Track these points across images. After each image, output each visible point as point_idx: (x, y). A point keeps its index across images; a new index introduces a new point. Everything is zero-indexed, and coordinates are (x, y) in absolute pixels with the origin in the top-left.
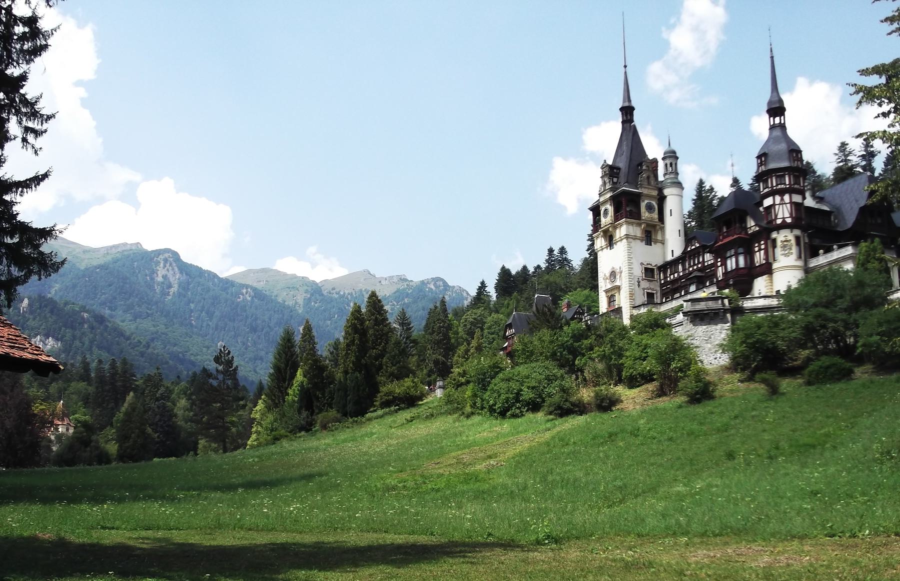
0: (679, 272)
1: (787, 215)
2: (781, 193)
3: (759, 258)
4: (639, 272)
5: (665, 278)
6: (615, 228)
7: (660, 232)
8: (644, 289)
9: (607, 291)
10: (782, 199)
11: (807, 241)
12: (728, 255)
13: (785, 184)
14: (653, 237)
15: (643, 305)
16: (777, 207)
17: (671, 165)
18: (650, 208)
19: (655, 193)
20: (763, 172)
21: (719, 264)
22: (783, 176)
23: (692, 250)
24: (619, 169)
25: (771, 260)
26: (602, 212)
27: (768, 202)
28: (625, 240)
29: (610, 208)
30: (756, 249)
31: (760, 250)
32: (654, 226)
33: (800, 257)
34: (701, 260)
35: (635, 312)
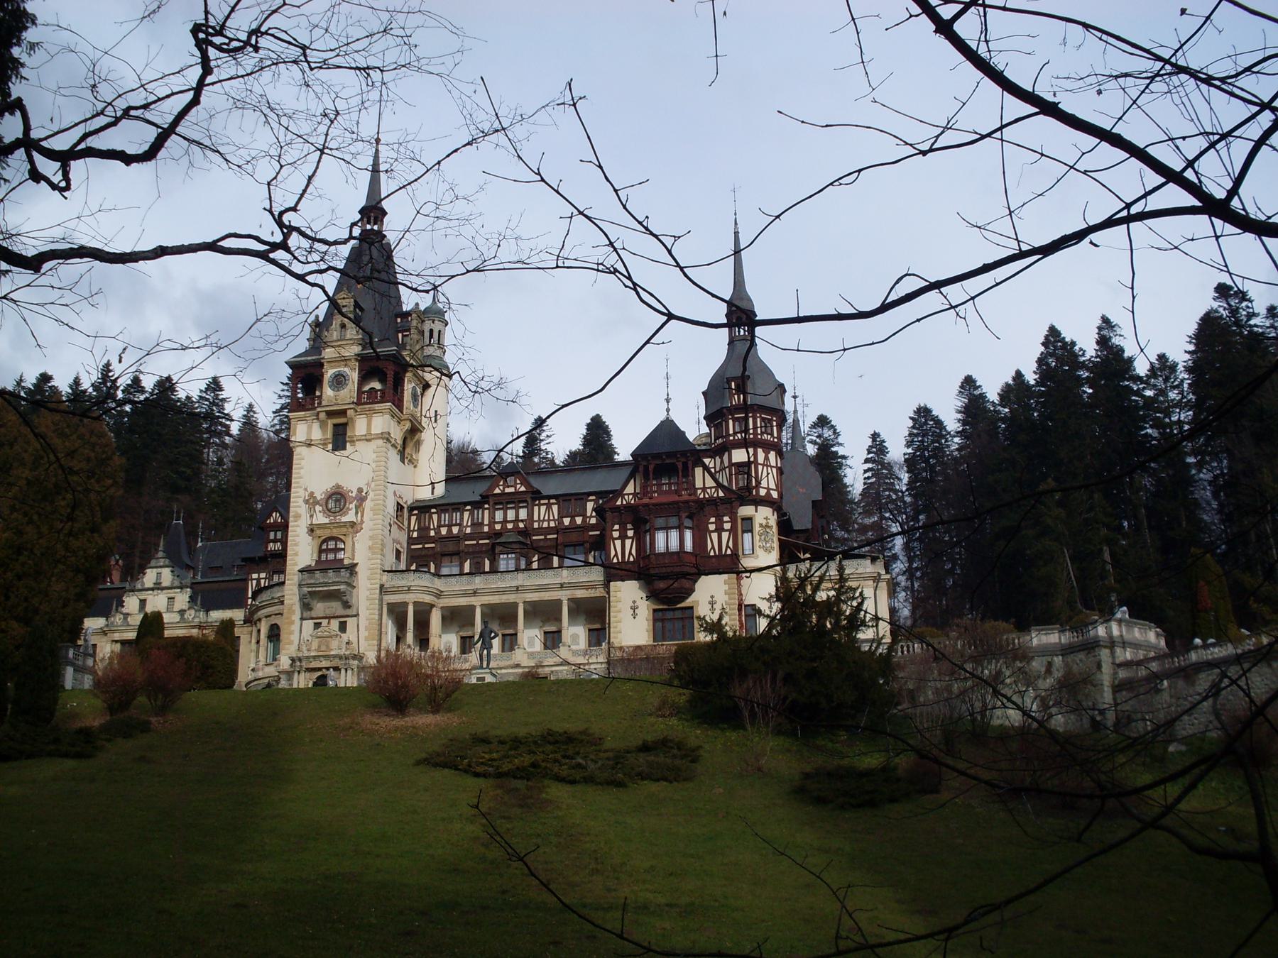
0: (460, 525)
1: (772, 486)
2: (768, 447)
5: (423, 530)
10: (766, 458)
13: (772, 434)
16: (760, 467)
18: (414, 397)
21: (616, 534)
22: (770, 421)
23: (503, 494)
24: (362, 310)
27: (739, 456)
28: (380, 442)
29: (354, 376)
30: (712, 527)
31: (720, 530)
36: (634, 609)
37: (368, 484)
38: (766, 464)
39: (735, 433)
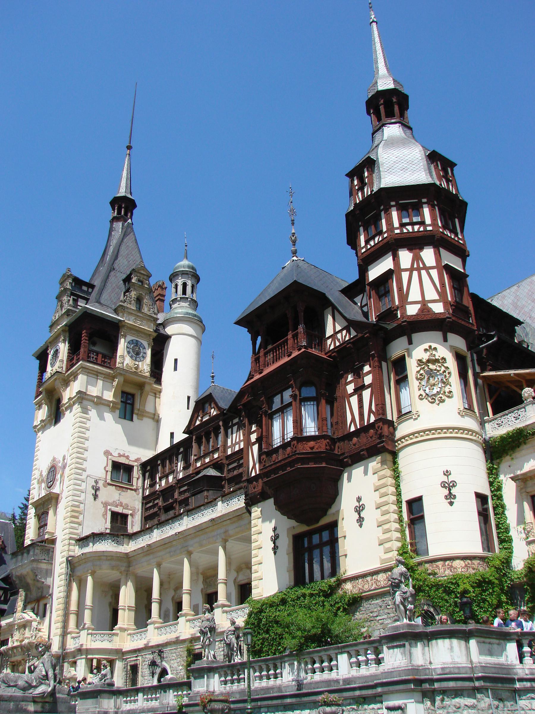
1: (431, 294)
2: (415, 243)
3: (357, 409)
4: (98, 468)
5: (152, 485)
6: (66, 383)
7: (150, 398)
8: (106, 504)
9: (37, 505)
10: (417, 258)
11: (478, 370)
12: (275, 407)
13: (422, 223)
14: (137, 405)
15: (96, 537)
16: (405, 276)
17: (185, 285)
19: (149, 328)
20: (366, 200)
23: (203, 424)
24: (92, 286)
25: (391, 414)
26: (50, 357)
32: (141, 386)
33: (470, 408)
34: (220, 444)
35: (77, 551)
36: (275, 539)
37: (68, 450)
38: (418, 266)
39: (367, 242)
